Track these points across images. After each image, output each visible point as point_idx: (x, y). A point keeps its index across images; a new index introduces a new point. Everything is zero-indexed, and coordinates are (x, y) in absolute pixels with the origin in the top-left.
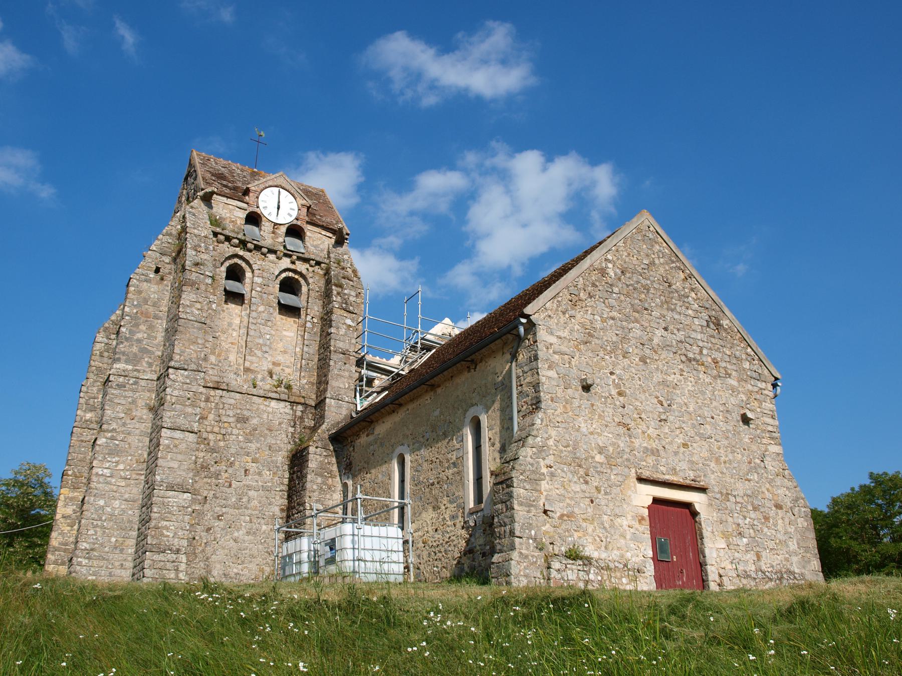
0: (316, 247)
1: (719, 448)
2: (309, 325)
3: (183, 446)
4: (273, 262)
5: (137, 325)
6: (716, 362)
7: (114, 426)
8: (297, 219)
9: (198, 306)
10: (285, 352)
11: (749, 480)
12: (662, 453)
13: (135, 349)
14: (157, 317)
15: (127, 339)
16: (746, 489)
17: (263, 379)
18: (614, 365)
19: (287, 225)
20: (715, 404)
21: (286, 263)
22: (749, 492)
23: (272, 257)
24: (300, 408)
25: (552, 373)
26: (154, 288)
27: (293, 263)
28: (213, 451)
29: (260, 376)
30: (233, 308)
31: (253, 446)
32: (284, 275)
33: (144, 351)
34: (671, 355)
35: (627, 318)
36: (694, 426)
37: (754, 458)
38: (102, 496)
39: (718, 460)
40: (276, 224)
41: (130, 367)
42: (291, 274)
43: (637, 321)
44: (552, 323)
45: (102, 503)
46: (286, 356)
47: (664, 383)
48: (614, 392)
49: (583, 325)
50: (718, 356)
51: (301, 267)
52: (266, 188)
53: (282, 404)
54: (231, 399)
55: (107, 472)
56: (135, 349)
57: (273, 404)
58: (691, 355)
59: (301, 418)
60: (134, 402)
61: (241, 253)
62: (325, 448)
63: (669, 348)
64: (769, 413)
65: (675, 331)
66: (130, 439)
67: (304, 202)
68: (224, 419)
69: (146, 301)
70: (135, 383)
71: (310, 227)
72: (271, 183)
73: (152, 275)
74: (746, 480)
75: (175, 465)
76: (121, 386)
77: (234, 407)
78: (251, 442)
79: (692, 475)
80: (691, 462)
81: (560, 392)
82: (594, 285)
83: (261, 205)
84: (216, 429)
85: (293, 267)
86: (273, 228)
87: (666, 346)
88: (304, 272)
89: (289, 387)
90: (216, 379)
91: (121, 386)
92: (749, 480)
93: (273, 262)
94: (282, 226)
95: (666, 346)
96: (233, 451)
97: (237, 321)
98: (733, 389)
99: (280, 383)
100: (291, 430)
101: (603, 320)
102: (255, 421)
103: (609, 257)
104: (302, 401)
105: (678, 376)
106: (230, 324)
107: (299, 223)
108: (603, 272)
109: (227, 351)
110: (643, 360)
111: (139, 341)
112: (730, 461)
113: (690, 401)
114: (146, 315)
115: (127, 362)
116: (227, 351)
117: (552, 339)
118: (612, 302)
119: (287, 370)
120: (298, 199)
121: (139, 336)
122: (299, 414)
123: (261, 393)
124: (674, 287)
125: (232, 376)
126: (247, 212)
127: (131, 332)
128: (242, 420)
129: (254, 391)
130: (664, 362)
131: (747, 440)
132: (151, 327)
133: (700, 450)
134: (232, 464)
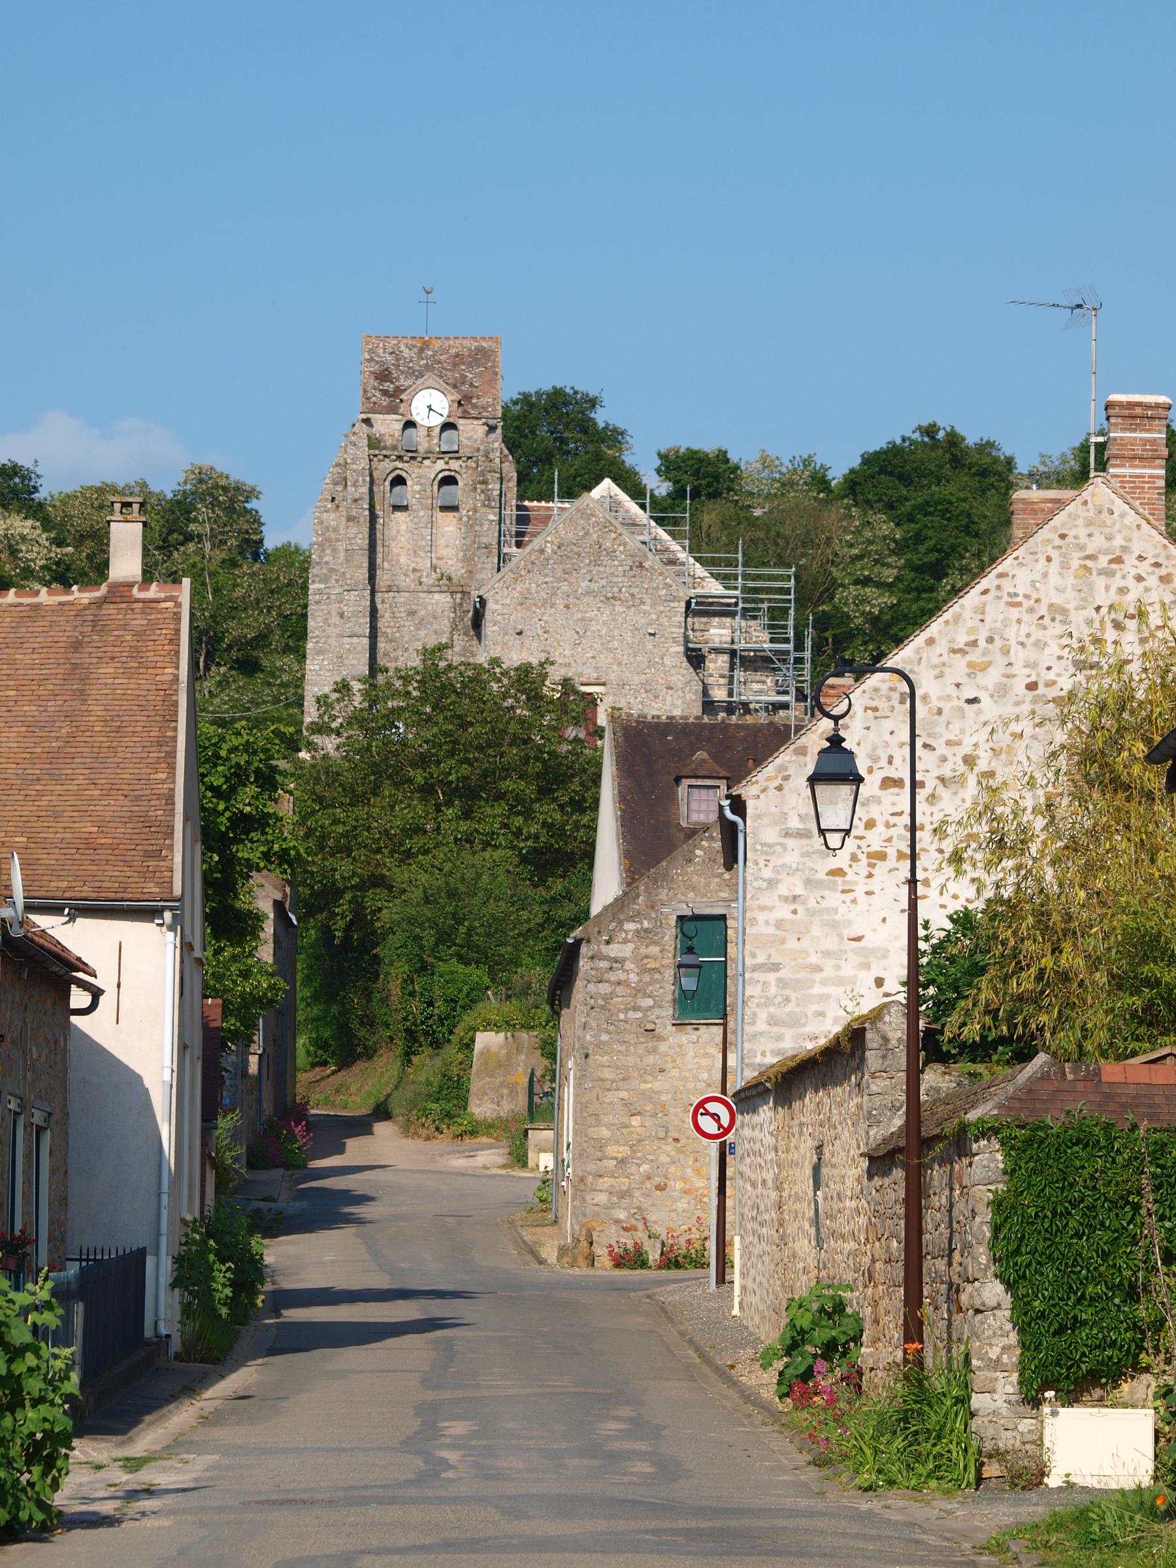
0: (469, 439)
2: (465, 519)
3: (359, 648)
4: (429, 467)
5: (323, 551)
6: (633, 595)
7: (317, 633)
8: (449, 416)
9: (360, 536)
10: (447, 546)
12: (573, 665)
13: (325, 571)
14: (338, 540)
15: (317, 563)
17: (428, 576)
18: (543, 614)
21: (440, 464)
23: (426, 462)
24: (459, 595)
25: (496, 628)
26: (332, 515)
27: (447, 463)
28: (391, 641)
29: (425, 574)
30: (399, 515)
31: (422, 633)
32: (440, 476)
33: (331, 570)
35: (559, 580)
36: (603, 644)
38: (316, 685)
39: (620, 664)
41: (322, 586)
42: (447, 473)
43: (565, 580)
44: (498, 597)
45: (316, 689)
46: (449, 549)
47: (583, 619)
48: (540, 632)
49: (521, 593)
50: (635, 590)
51: (455, 465)
53: (443, 595)
54: (401, 598)
55: (317, 667)
56: (325, 571)
57: (436, 596)
58: (610, 595)
59: (461, 604)
60: (329, 613)
61: (400, 465)
62: (466, 634)
66: (330, 641)
67: (453, 398)
68: (397, 615)
69: (327, 529)
70: (328, 598)
71: (461, 421)
73: (329, 506)
75: (355, 662)
76: (317, 603)
77: (404, 603)
78: (419, 630)
79: (595, 675)
80: (597, 668)
81: (500, 639)
82: (533, 563)
83: (414, 413)
84: (392, 624)
85: (447, 467)
87: (588, 593)
88: (458, 469)
89: (450, 579)
90: (389, 583)
91: (317, 603)
93: (429, 467)
95: (588, 593)
96: (406, 639)
97: (404, 527)
98: (645, 612)
99: (442, 575)
100: (452, 615)
101: (538, 586)
102: (422, 613)
103: (549, 539)
104: (460, 589)
105: (595, 612)
106: (398, 531)
107: (451, 420)
108: (542, 551)
109: (398, 555)
110: (567, 607)
111: (327, 563)
114: (329, 540)
115: (320, 582)
116: (398, 555)
117: (498, 607)
118: (546, 571)
119: (450, 562)
121: (326, 559)
122: (458, 601)
123: (425, 588)
125: (402, 577)
127: (321, 557)
128: (412, 613)
129: (420, 588)
132: (335, 550)
133: (604, 659)
134: (406, 650)
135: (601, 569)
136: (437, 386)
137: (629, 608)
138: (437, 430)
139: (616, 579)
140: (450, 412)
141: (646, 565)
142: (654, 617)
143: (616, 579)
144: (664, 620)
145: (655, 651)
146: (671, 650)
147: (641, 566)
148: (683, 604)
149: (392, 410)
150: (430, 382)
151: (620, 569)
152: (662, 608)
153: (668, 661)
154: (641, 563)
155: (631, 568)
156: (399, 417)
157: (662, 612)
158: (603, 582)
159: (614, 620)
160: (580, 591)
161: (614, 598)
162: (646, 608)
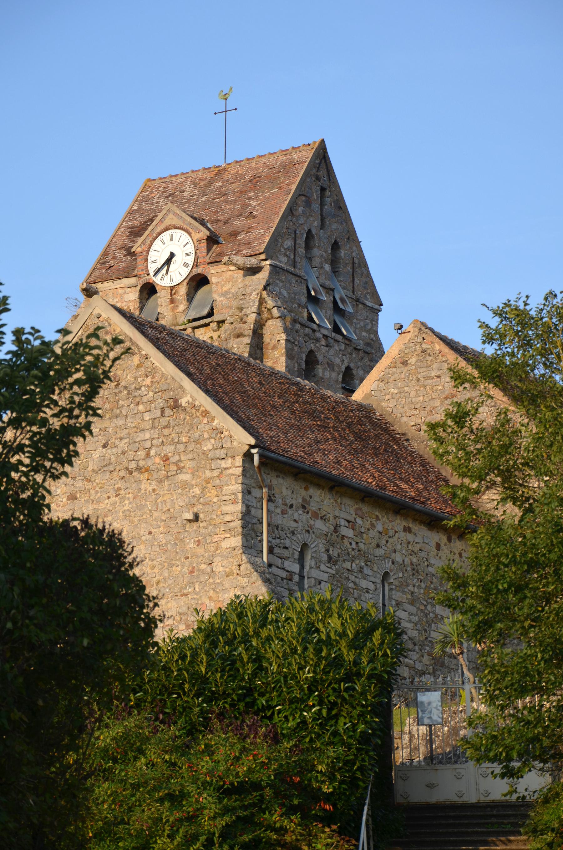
0: (224, 294)
1: (153, 568)
6: (166, 459)
8: (196, 265)
11: (185, 595)
16: (181, 607)
19: (186, 281)
20: (155, 514)
22: (184, 609)
34: (107, 475)
37: (199, 564)
40: (172, 288)
50: (169, 450)
52: (155, 239)
63: (105, 469)
64: (230, 497)
65: (117, 443)
72: (159, 229)
74: (182, 596)
86: (171, 296)
92: (185, 595)
94: (180, 286)
98: (185, 485)
107: (199, 270)
112: (165, 579)
113: (123, 523)
120: (193, 235)
124: (123, 383)
126: (138, 288)
130: (97, 489)
131: (191, 545)
135: (120, 422)
136: (178, 223)
137: (161, 481)
138: (183, 290)
139: (140, 436)
140: (197, 258)
141: (183, 402)
142: (197, 491)
143: (140, 436)
144: (211, 495)
145: (200, 551)
146: (225, 545)
147: (176, 406)
148: (239, 461)
149: (127, 273)
150: (171, 220)
151: (147, 416)
152: (208, 474)
153: (218, 568)
154: (176, 401)
155: (163, 412)
156: (132, 281)
157: (208, 481)
158: (123, 445)
159: (141, 507)
160: (91, 466)
161: (139, 469)
162: (185, 477)
